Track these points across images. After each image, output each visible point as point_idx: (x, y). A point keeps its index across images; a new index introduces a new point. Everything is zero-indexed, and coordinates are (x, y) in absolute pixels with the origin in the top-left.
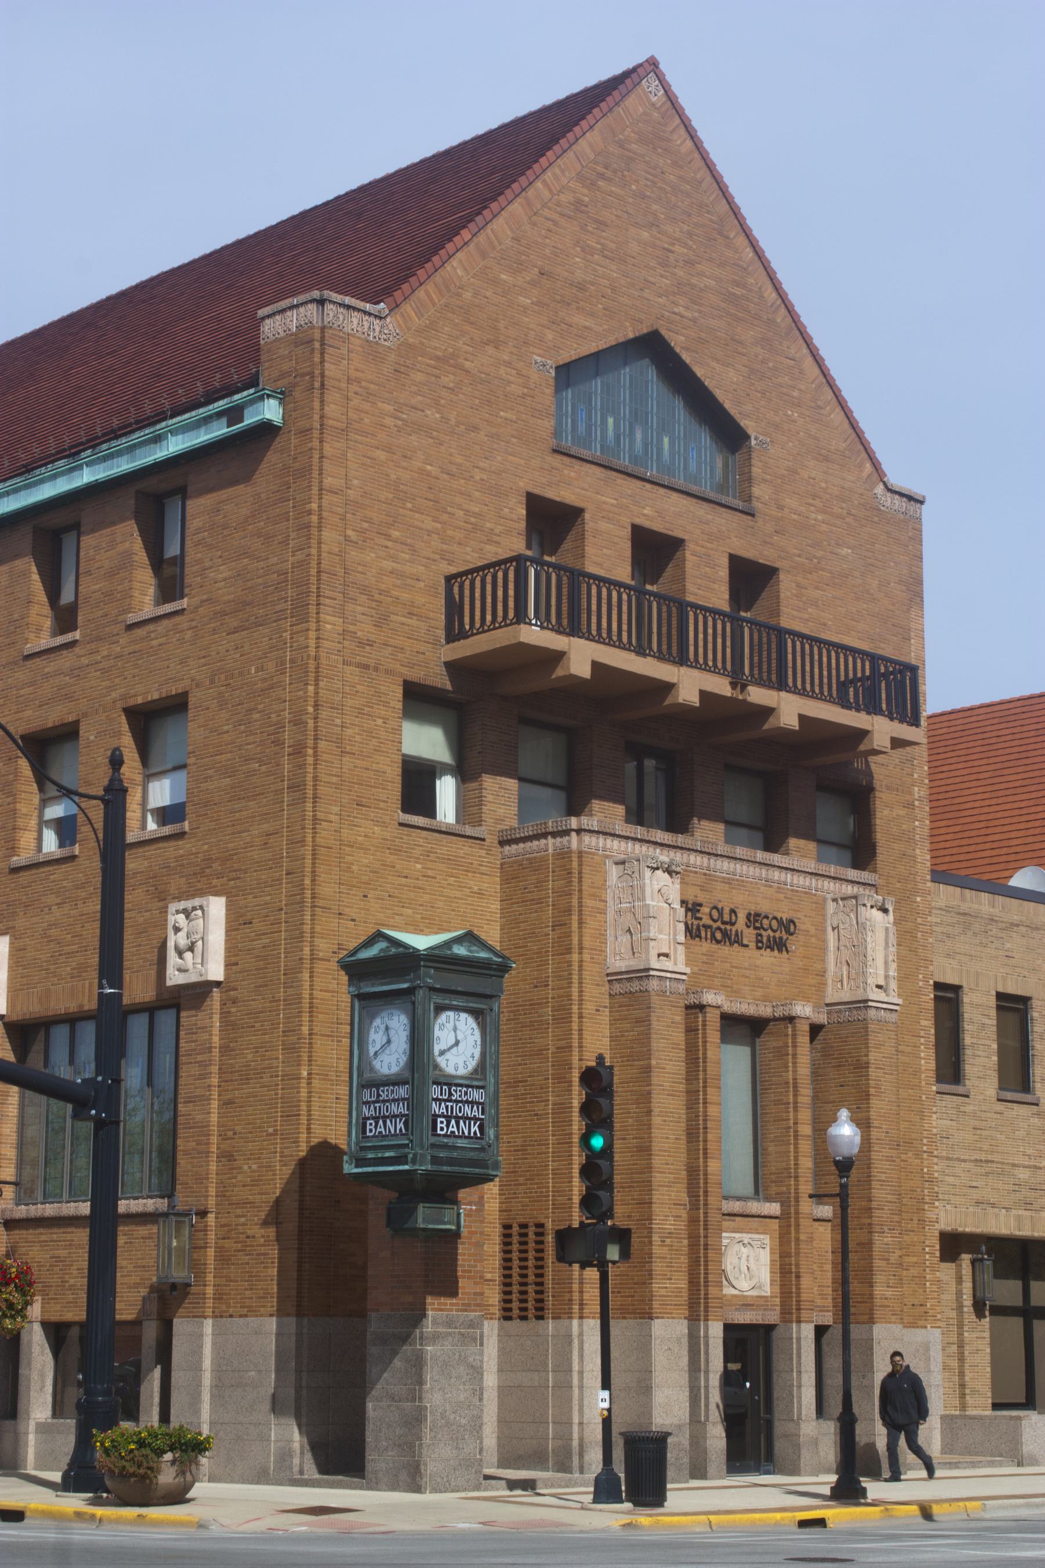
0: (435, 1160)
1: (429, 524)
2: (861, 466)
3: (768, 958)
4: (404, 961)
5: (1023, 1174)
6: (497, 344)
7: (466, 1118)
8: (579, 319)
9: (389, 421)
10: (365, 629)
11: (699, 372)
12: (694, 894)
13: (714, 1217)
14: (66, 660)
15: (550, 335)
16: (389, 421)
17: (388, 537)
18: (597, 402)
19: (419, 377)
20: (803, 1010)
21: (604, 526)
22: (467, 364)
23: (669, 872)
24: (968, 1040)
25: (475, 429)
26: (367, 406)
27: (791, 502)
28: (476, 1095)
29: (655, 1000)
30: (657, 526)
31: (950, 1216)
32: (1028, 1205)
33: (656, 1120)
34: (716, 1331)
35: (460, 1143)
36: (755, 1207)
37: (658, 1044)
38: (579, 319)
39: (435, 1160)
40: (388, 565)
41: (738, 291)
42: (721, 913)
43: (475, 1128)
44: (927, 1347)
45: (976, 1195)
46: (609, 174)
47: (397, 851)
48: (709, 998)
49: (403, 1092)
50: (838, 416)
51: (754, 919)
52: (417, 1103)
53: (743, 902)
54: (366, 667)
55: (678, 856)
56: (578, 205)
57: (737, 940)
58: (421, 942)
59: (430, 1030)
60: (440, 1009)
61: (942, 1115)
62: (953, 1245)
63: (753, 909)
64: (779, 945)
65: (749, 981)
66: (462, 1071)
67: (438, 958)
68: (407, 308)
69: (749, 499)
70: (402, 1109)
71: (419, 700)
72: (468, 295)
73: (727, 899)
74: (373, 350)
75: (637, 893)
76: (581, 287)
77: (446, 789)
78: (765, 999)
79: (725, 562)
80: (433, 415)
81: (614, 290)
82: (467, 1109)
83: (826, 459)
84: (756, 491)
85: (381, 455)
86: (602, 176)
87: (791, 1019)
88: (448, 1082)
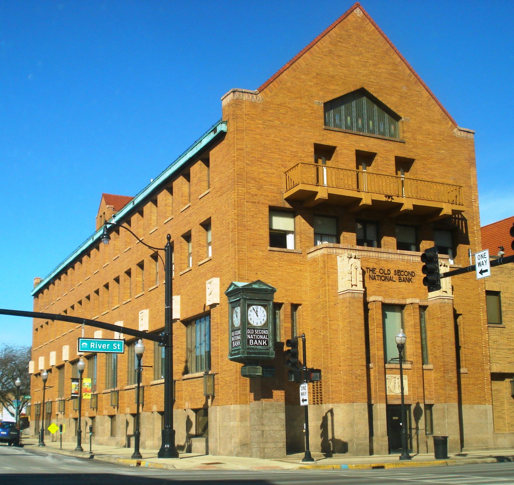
0: (248, 353)
1: (277, 156)
2: (447, 123)
3: (403, 285)
6: (301, 98)
7: (260, 340)
8: (332, 87)
9: (260, 126)
10: (254, 191)
14: (189, 212)
15: (321, 93)
16: (260, 126)
17: (261, 161)
18: (343, 113)
19: (271, 111)
21: (345, 151)
22: (290, 106)
25: (293, 125)
26: (252, 122)
27: (419, 137)
30: (366, 149)
31: (496, 369)
35: (259, 347)
38: (332, 87)
39: (248, 353)
40: (262, 170)
41: (394, 72)
42: (384, 272)
43: (265, 343)
44: (486, 411)
45: (509, 360)
46: (342, 40)
47: (268, 259)
49: (239, 332)
51: (398, 272)
53: (393, 267)
54: (255, 202)
56: (330, 52)
57: (391, 279)
60: (249, 306)
62: (497, 377)
63: (397, 269)
64: (409, 280)
66: (259, 325)
67: (244, 289)
72: (289, 84)
73: (386, 267)
74: (253, 105)
76: (333, 77)
79: (394, 159)
80: (277, 123)
81: (345, 77)
82: (261, 337)
83: (433, 122)
85: (258, 137)
86: (339, 42)
88: (254, 328)
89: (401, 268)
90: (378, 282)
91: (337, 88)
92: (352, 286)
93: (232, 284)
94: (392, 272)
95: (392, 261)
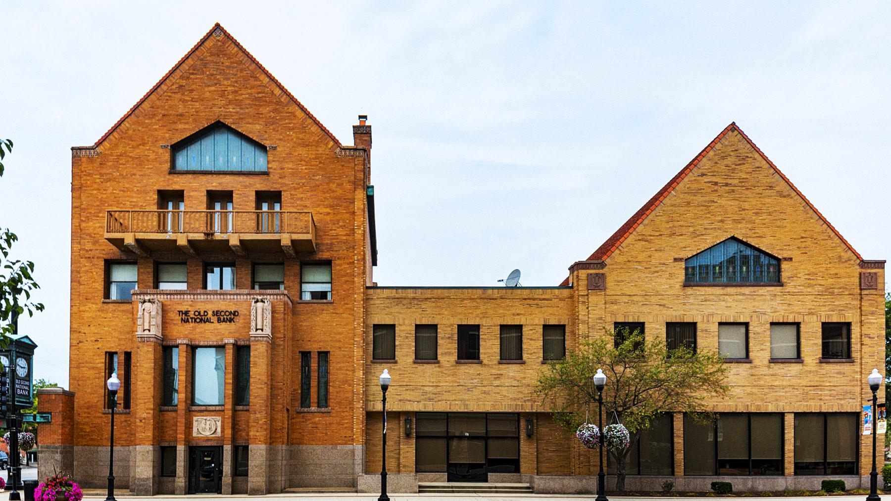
2: (327, 144)
3: (223, 325)
6: (144, 144)
8: (181, 126)
9: (98, 181)
10: (88, 246)
16: (98, 181)
19: (110, 164)
25: (134, 174)
38: (181, 126)
41: (260, 95)
42: (199, 313)
50: (314, 128)
51: (216, 313)
57: (208, 321)
63: (215, 310)
64: (231, 320)
73: (202, 308)
76: (181, 115)
80: (116, 174)
81: (197, 112)
83: (308, 145)
86: (193, 74)
90: (192, 325)
91: (187, 126)
94: (210, 313)
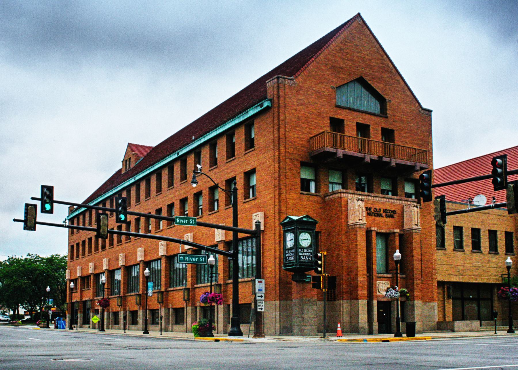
3: (388, 220)
4: (292, 222)
5: (460, 268)
7: (307, 256)
8: (342, 76)
11: (373, 85)
12: (369, 206)
13: (374, 277)
17: (296, 130)
20: (397, 231)
22: (314, 89)
23: (362, 200)
24: (446, 237)
26: (290, 100)
28: (310, 251)
29: (358, 230)
31: (440, 278)
32: (461, 274)
33: (359, 256)
34: (375, 302)
35: (307, 261)
36: (385, 275)
37: (359, 239)
38: (342, 76)
40: (296, 136)
41: (382, 65)
43: (310, 258)
44: (434, 307)
45: (449, 272)
48: (373, 229)
49: (293, 251)
50: (409, 93)
51: (385, 211)
52: (296, 253)
53: (382, 207)
54: (291, 159)
55: (364, 197)
57: (380, 216)
58: (295, 218)
59: (299, 237)
60: (301, 233)
61: (439, 255)
64: (392, 217)
65: (384, 224)
66: (307, 246)
67: (299, 221)
68: (299, 78)
69: (386, 114)
70: (293, 254)
71: (304, 164)
75: (354, 206)
77: (313, 185)
78: (388, 229)
81: (350, 68)
82: (308, 254)
84: (388, 112)
85: (294, 111)
87: (394, 233)
88: (303, 248)
89: (388, 208)
90: (373, 217)
92: (359, 220)
93: (287, 217)
94: (382, 210)
95: (382, 203)
